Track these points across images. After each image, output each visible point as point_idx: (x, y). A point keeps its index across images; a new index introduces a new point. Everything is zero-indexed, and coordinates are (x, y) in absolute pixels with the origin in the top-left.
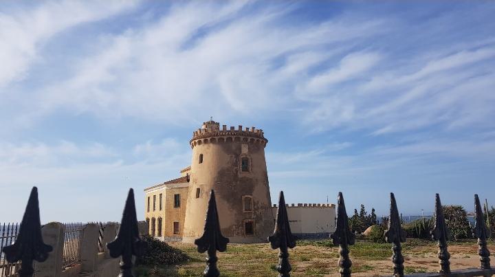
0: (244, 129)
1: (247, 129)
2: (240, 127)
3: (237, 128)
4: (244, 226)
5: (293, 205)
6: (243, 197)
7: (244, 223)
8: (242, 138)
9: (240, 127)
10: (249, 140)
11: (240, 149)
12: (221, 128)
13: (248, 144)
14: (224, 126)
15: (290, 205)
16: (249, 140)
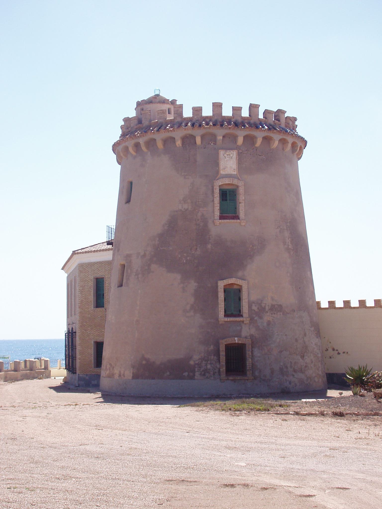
0: (227, 112)
1: (236, 110)
2: (217, 106)
3: (207, 112)
4: (223, 354)
5: (332, 303)
6: (221, 284)
7: (222, 348)
8: (220, 133)
9: (217, 106)
10: (240, 141)
11: (216, 163)
12: (187, 113)
13: (237, 148)
14: (266, 112)
15: (325, 305)
16: (240, 141)
